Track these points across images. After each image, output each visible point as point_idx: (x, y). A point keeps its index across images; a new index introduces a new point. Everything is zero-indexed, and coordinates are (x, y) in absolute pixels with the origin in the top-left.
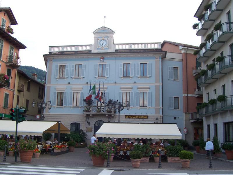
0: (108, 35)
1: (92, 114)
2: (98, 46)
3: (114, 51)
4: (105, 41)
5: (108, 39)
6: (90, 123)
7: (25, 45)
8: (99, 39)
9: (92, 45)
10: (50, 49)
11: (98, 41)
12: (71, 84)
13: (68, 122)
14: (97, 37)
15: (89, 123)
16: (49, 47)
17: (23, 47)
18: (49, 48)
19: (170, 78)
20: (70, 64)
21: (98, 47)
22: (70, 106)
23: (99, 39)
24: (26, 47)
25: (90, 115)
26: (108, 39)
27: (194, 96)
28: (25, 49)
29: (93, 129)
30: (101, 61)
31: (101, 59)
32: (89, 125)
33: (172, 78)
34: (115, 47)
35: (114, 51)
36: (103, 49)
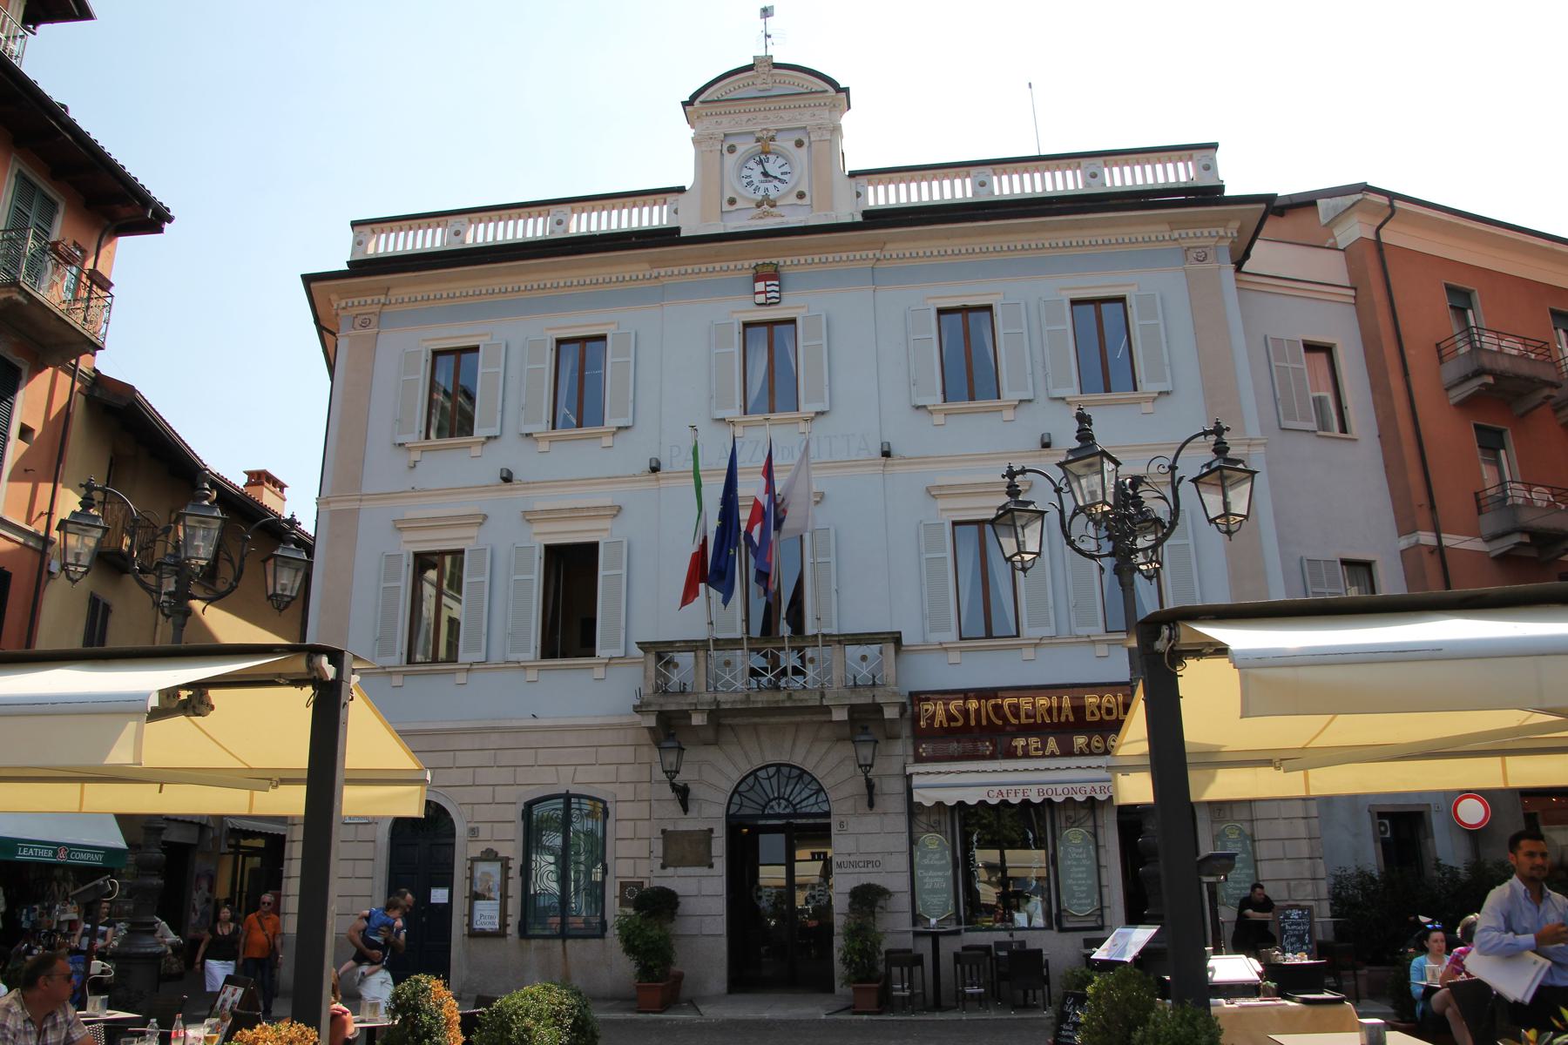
0: (806, 119)
1: (711, 711)
2: (728, 195)
3: (859, 218)
4: (781, 161)
5: (799, 144)
6: (696, 791)
7: (160, 191)
8: (732, 149)
9: (681, 190)
10: (358, 243)
11: (730, 160)
12: (528, 485)
13: (503, 794)
14: (719, 132)
15: (683, 795)
16: (354, 224)
17: (144, 215)
18: (349, 234)
19: (1290, 415)
20: (514, 345)
21: (732, 201)
22: (513, 657)
23: (732, 149)
24: (170, 219)
25: (698, 720)
26: (799, 144)
27: (1476, 545)
28: (160, 231)
29: (719, 847)
30: (761, 298)
31: (760, 286)
32: (686, 810)
33: (1306, 419)
34: (858, 195)
35: (859, 218)
36: (766, 215)
